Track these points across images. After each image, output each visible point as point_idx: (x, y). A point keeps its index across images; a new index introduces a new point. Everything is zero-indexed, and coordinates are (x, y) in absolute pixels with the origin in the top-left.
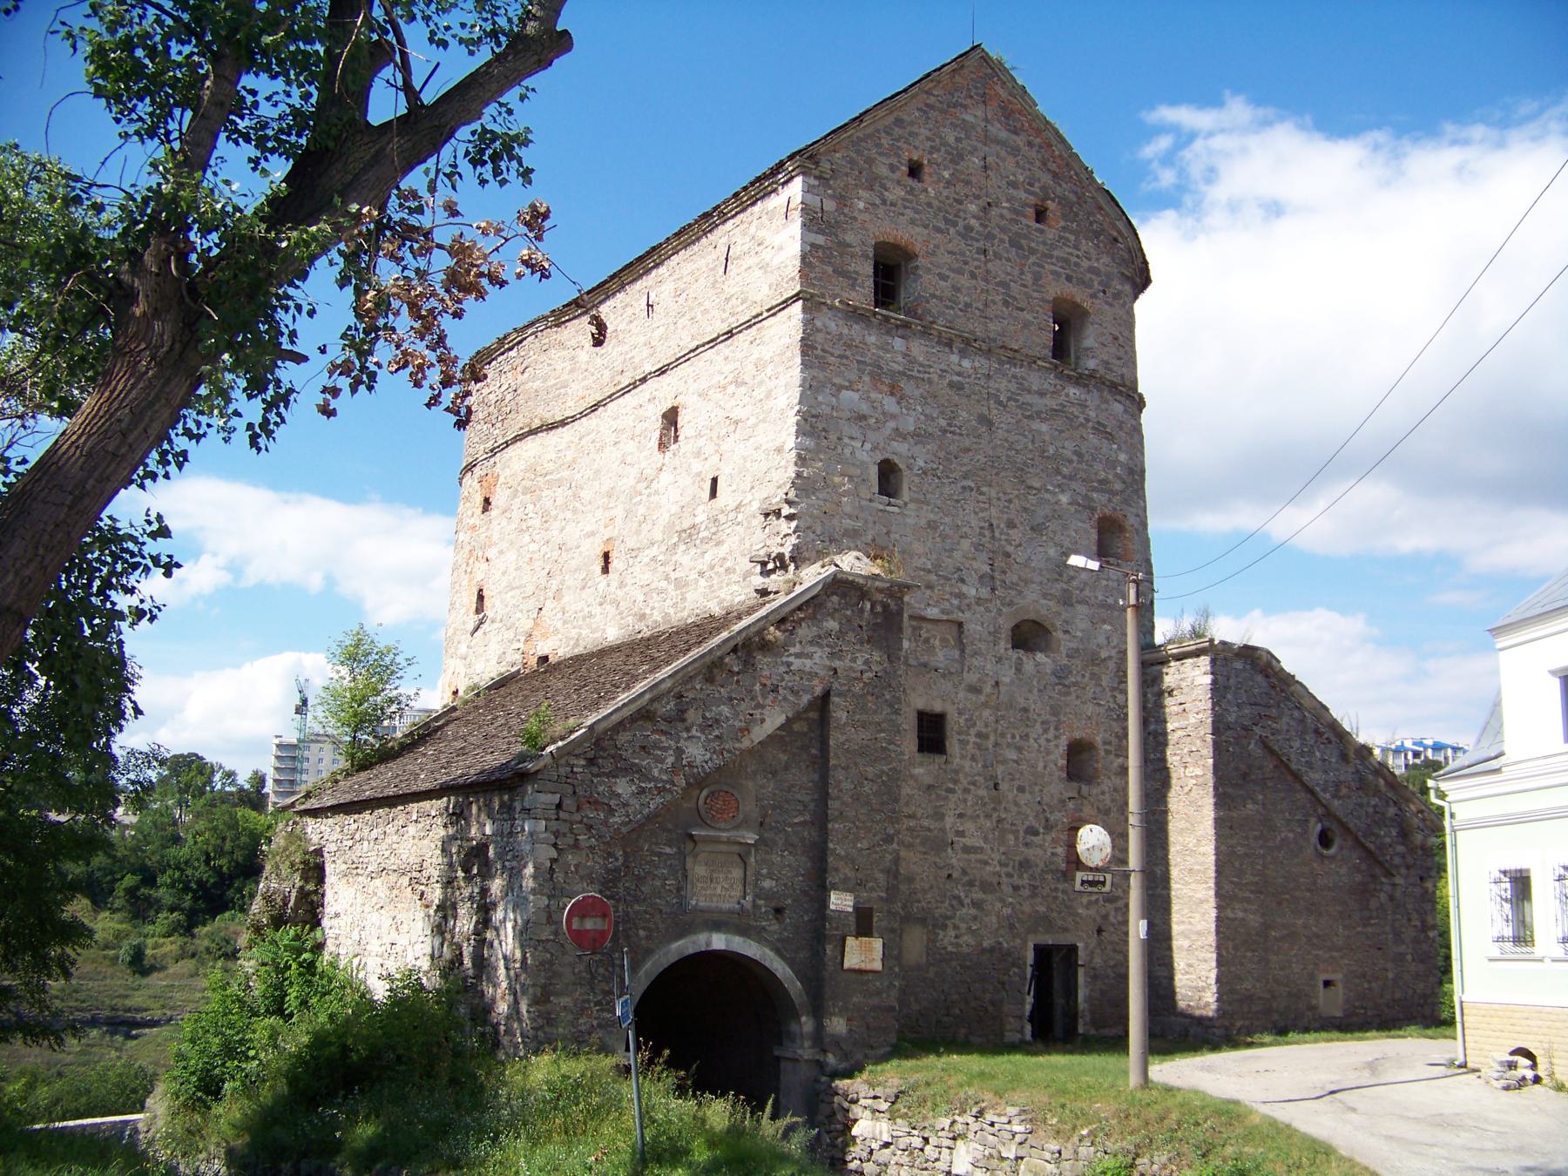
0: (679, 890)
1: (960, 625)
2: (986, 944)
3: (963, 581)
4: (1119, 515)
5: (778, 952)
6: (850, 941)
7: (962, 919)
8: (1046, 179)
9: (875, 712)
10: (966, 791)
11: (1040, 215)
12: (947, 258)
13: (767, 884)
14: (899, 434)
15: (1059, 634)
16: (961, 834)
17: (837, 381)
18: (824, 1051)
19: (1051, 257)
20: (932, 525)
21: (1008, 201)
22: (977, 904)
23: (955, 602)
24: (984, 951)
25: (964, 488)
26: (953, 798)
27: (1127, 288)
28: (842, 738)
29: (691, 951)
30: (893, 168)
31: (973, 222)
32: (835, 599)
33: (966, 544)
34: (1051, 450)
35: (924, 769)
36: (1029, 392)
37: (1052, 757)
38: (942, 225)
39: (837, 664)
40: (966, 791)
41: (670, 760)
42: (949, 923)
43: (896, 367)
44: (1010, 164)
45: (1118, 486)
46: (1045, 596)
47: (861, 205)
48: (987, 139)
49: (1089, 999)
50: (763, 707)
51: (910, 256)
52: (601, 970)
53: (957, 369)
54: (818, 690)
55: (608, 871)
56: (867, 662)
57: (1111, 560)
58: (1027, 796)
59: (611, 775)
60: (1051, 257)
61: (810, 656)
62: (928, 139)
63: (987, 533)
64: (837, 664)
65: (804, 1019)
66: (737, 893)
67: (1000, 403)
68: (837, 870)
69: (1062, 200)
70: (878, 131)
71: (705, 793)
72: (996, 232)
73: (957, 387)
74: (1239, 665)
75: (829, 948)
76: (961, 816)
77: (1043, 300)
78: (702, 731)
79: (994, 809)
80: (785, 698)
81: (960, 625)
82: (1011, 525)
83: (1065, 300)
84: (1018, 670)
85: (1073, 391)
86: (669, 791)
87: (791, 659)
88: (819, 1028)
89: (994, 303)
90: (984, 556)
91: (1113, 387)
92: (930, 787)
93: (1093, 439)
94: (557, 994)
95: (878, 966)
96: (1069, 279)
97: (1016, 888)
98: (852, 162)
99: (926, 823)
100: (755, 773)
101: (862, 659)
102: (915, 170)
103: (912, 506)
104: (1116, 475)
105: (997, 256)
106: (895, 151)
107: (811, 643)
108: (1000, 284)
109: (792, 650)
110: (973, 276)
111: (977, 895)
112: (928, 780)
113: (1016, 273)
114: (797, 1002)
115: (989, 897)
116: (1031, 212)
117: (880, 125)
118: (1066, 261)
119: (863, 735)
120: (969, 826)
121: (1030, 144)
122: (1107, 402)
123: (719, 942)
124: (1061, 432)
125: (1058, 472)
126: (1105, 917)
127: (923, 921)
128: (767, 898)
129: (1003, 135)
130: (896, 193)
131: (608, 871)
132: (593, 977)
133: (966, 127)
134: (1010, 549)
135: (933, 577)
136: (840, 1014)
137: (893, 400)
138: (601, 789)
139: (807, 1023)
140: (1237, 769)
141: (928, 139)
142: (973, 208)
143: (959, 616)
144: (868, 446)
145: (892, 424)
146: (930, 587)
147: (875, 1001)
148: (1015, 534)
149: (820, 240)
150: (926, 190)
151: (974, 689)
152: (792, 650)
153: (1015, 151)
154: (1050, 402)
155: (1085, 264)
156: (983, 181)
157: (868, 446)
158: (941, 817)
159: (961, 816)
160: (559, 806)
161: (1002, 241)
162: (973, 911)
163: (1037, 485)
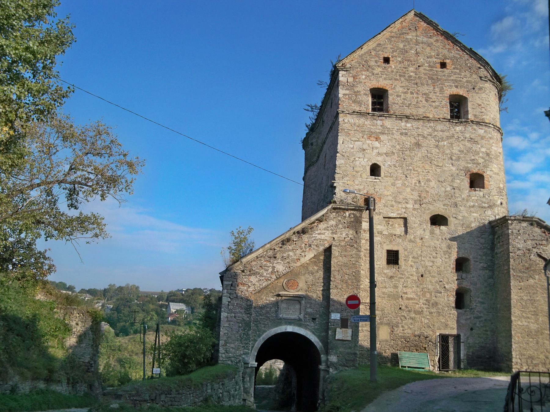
0: (276, 311)
1: (405, 219)
2: (417, 333)
3: (407, 203)
4: (480, 172)
5: (313, 333)
6: (338, 330)
7: (406, 324)
8: (445, 52)
9: (350, 251)
10: (407, 278)
11: (443, 65)
12: (401, 89)
13: (309, 310)
14: (379, 154)
15: (451, 220)
16: (406, 293)
17: (353, 139)
18: (329, 367)
19: (448, 80)
20: (393, 184)
21: (427, 63)
22: (412, 318)
23: (404, 210)
24: (415, 336)
25: (407, 170)
26: (403, 280)
27: (488, 86)
28: (336, 261)
29: (279, 332)
30: (376, 62)
31: (412, 74)
32: (334, 214)
33: (408, 190)
34: (448, 151)
35: (391, 270)
36: (437, 131)
37: (448, 264)
38: (398, 78)
39: (334, 236)
40: (407, 278)
41: (270, 270)
42: (400, 325)
43: (378, 131)
44: (428, 49)
45: (481, 161)
46: (444, 205)
47: (364, 77)
48: (417, 43)
49: (467, 355)
50: (305, 252)
51: (385, 91)
52: (245, 336)
53: (405, 127)
54: (327, 245)
55: (247, 306)
56: (347, 234)
57: (477, 189)
58: (436, 279)
59: (250, 275)
60: (448, 80)
61: (324, 234)
62: (391, 48)
63: (417, 184)
64: (334, 236)
65: (322, 356)
66: (298, 313)
67: (424, 137)
68: (333, 305)
69: (453, 59)
70: (370, 50)
71: (286, 280)
72: (422, 76)
73: (406, 134)
74: (524, 224)
75: (330, 332)
76: (405, 287)
77: (444, 97)
78: (282, 261)
79: (421, 284)
80: (314, 249)
81: (405, 219)
82: (429, 180)
83: (455, 95)
84: (432, 233)
85: (459, 128)
86: (270, 280)
87: (316, 235)
88: (328, 359)
89: (421, 101)
90: (416, 194)
91: (478, 123)
92: (391, 277)
93: (468, 145)
94: (229, 343)
95: (349, 338)
96: (457, 87)
97: (431, 313)
98: (359, 63)
99: (392, 290)
100: (304, 274)
101: (346, 234)
102: (387, 60)
103: (385, 178)
104: (480, 157)
105: (422, 84)
106: (377, 55)
107: (324, 229)
108: (425, 94)
109: (317, 232)
110: (412, 93)
111: (413, 315)
112: (391, 274)
113: (432, 88)
114: (319, 350)
115: (418, 316)
116: (439, 65)
117: (371, 48)
118: (456, 81)
119: (345, 260)
120: (409, 290)
121: (437, 41)
122: (475, 130)
123: (290, 329)
124: (452, 144)
125: (452, 159)
126: (475, 324)
127: (388, 324)
128: (309, 315)
129: (425, 39)
130: (378, 70)
131: (247, 306)
132: (242, 338)
133: (408, 41)
134: (428, 189)
135: (393, 203)
136: (336, 354)
137: (377, 142)
138: (245, 280)
139: (323, 357)
140: (523, 266)
141: (391, 48)
142: (411, 69)
143: (406, 216)
144: (366, 160)
145: (375, 151)
146: (392, 206)
147: (349, 351)
148: (432, 184)
149: (347, 92)
150: (391, 67)
151: (410, 241)
152: (317, 232)
153: (429, 45)
154: (447, 134)
155: (465, 79)
156: (415, 58)
157: (366, 160)
158: (396, 287)
159: (405, 287)
160: (232, 285)
161: (426, 78)
162: (410, 321)
163: (441, 165)
